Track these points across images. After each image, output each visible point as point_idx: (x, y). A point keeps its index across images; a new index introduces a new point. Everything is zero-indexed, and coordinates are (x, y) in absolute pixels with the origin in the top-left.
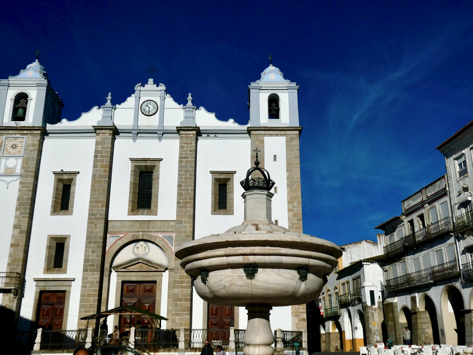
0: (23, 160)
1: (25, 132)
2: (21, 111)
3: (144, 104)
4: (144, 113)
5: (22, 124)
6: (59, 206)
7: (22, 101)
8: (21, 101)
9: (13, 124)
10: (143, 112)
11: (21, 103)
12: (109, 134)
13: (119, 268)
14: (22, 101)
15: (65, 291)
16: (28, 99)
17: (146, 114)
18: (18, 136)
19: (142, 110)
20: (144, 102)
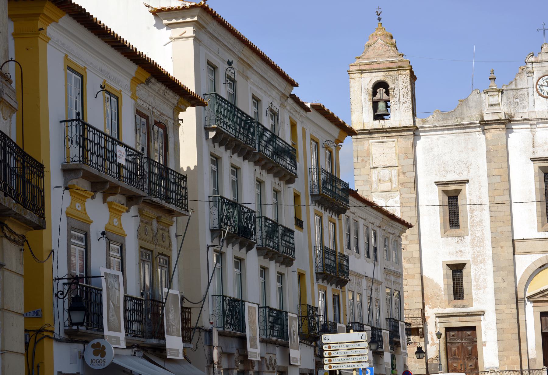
0: (398, 170)
1: (394, 134)
2: (381, 105)
3: (540, 81)
4: (542, 94)
5: (386, 124)
6: (448, 225)
7: (380, 90)
8: (378, 90)
9: (377, 124)
10: (540, 92)
11: (379, 93)
12: (501, 129)
13: (534, 297)
14: (380, 90)
15: (473, 328)
16: (389, 88)
17: (544, 95)
18: (385, 139)
19: (539, 90)
20: (539, 79)
